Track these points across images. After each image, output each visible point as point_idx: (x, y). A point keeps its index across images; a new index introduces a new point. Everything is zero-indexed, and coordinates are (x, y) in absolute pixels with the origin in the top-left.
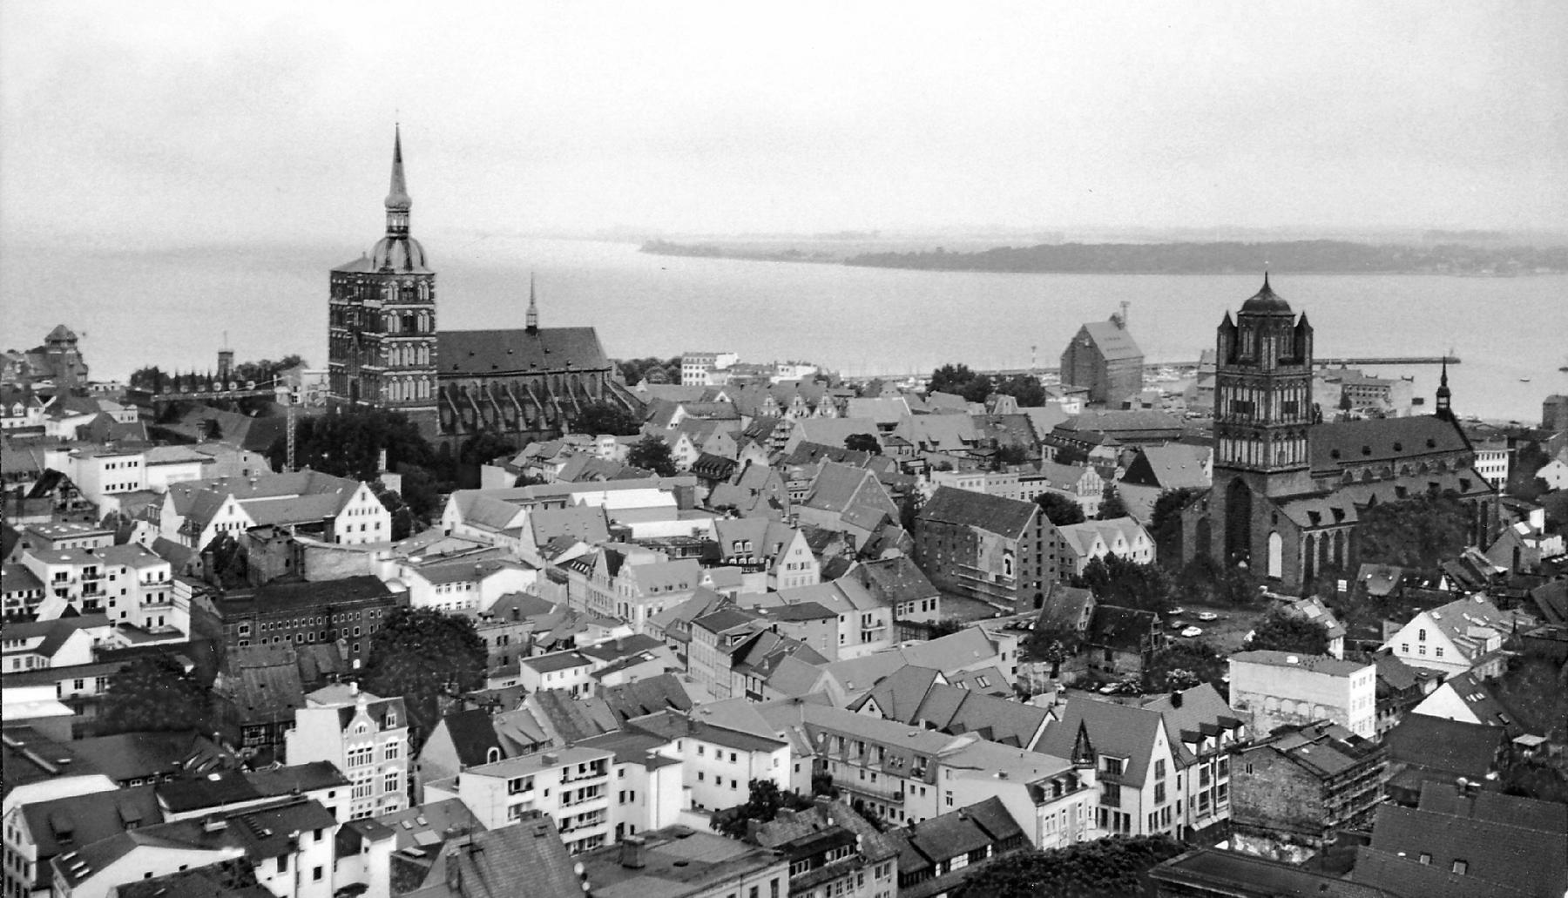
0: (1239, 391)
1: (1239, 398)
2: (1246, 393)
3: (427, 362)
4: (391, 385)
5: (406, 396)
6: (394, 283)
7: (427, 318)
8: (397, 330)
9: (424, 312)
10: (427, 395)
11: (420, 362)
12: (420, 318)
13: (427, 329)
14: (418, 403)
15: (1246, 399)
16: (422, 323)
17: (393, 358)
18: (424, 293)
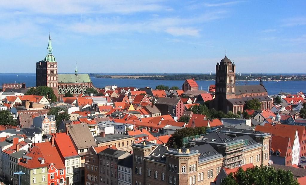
0: (220, 78)
1: (220, 79)
2: (222, 78)
3: (56, 80)
4: (49, 84)
5: (51, 86)
6: (49, 64)
7: (56, 71)
8: (50, 73)
9: (55, 70)
10: (56, 86)
11: (54, 80)
12: (54, 71)
13: (56, 73)
14: (55, 88)
15: (222, 79)
16: (55, 72)
17: (49, 78)
18: (55, 66)
